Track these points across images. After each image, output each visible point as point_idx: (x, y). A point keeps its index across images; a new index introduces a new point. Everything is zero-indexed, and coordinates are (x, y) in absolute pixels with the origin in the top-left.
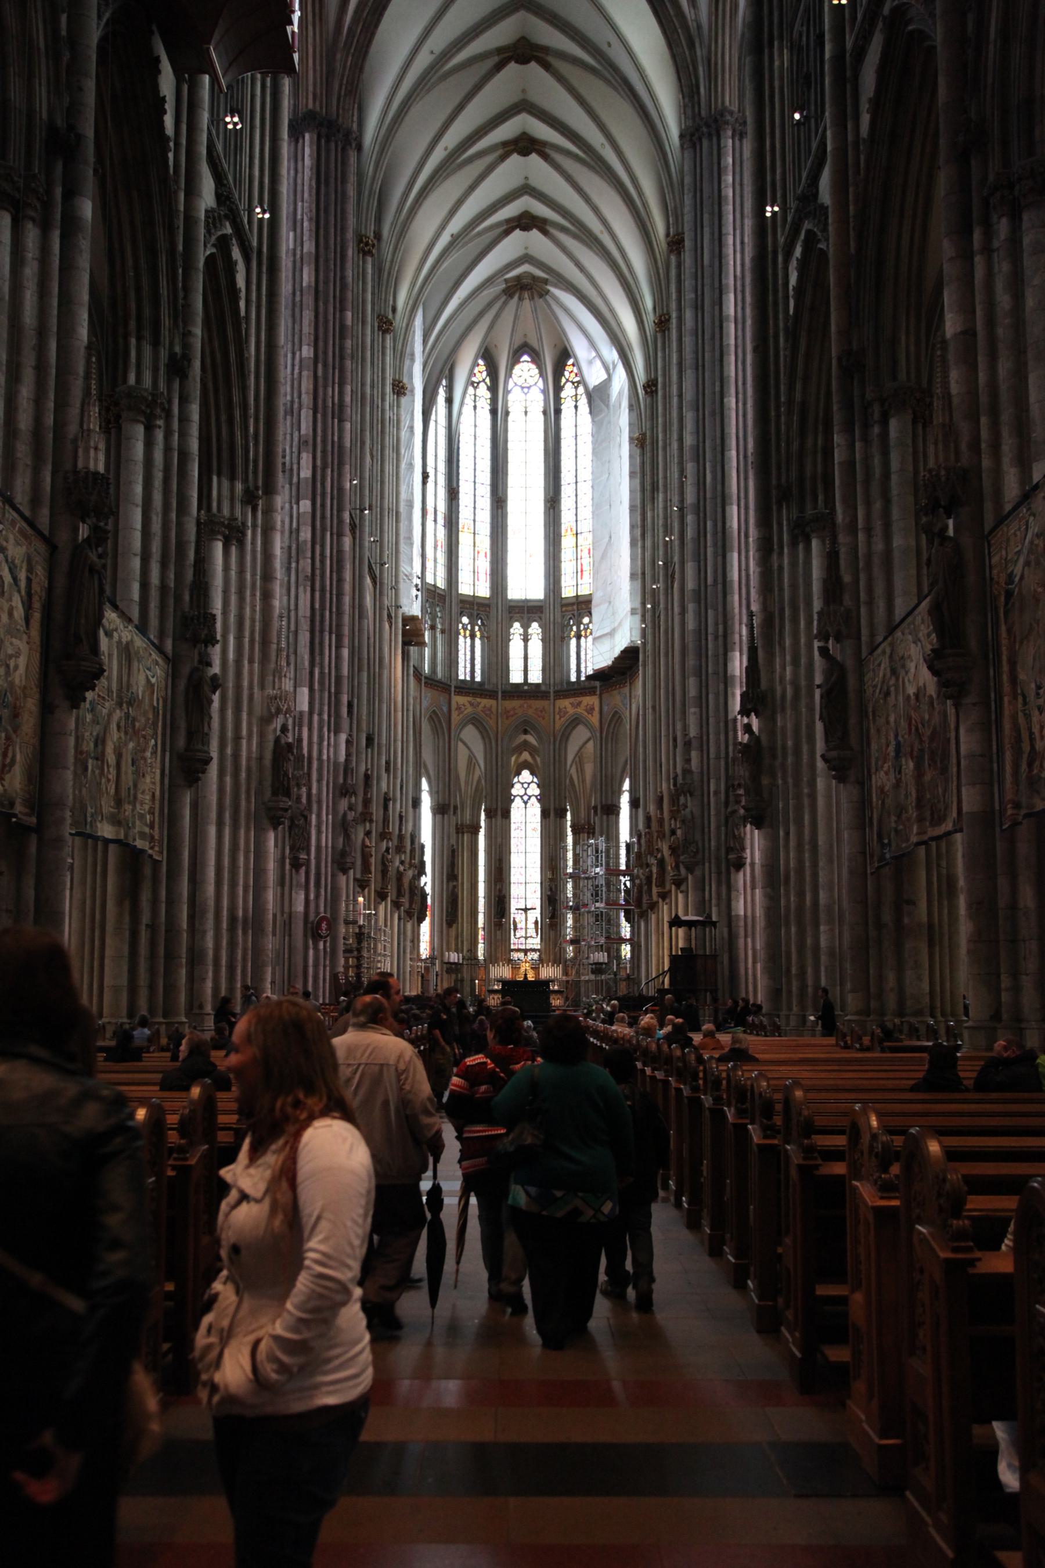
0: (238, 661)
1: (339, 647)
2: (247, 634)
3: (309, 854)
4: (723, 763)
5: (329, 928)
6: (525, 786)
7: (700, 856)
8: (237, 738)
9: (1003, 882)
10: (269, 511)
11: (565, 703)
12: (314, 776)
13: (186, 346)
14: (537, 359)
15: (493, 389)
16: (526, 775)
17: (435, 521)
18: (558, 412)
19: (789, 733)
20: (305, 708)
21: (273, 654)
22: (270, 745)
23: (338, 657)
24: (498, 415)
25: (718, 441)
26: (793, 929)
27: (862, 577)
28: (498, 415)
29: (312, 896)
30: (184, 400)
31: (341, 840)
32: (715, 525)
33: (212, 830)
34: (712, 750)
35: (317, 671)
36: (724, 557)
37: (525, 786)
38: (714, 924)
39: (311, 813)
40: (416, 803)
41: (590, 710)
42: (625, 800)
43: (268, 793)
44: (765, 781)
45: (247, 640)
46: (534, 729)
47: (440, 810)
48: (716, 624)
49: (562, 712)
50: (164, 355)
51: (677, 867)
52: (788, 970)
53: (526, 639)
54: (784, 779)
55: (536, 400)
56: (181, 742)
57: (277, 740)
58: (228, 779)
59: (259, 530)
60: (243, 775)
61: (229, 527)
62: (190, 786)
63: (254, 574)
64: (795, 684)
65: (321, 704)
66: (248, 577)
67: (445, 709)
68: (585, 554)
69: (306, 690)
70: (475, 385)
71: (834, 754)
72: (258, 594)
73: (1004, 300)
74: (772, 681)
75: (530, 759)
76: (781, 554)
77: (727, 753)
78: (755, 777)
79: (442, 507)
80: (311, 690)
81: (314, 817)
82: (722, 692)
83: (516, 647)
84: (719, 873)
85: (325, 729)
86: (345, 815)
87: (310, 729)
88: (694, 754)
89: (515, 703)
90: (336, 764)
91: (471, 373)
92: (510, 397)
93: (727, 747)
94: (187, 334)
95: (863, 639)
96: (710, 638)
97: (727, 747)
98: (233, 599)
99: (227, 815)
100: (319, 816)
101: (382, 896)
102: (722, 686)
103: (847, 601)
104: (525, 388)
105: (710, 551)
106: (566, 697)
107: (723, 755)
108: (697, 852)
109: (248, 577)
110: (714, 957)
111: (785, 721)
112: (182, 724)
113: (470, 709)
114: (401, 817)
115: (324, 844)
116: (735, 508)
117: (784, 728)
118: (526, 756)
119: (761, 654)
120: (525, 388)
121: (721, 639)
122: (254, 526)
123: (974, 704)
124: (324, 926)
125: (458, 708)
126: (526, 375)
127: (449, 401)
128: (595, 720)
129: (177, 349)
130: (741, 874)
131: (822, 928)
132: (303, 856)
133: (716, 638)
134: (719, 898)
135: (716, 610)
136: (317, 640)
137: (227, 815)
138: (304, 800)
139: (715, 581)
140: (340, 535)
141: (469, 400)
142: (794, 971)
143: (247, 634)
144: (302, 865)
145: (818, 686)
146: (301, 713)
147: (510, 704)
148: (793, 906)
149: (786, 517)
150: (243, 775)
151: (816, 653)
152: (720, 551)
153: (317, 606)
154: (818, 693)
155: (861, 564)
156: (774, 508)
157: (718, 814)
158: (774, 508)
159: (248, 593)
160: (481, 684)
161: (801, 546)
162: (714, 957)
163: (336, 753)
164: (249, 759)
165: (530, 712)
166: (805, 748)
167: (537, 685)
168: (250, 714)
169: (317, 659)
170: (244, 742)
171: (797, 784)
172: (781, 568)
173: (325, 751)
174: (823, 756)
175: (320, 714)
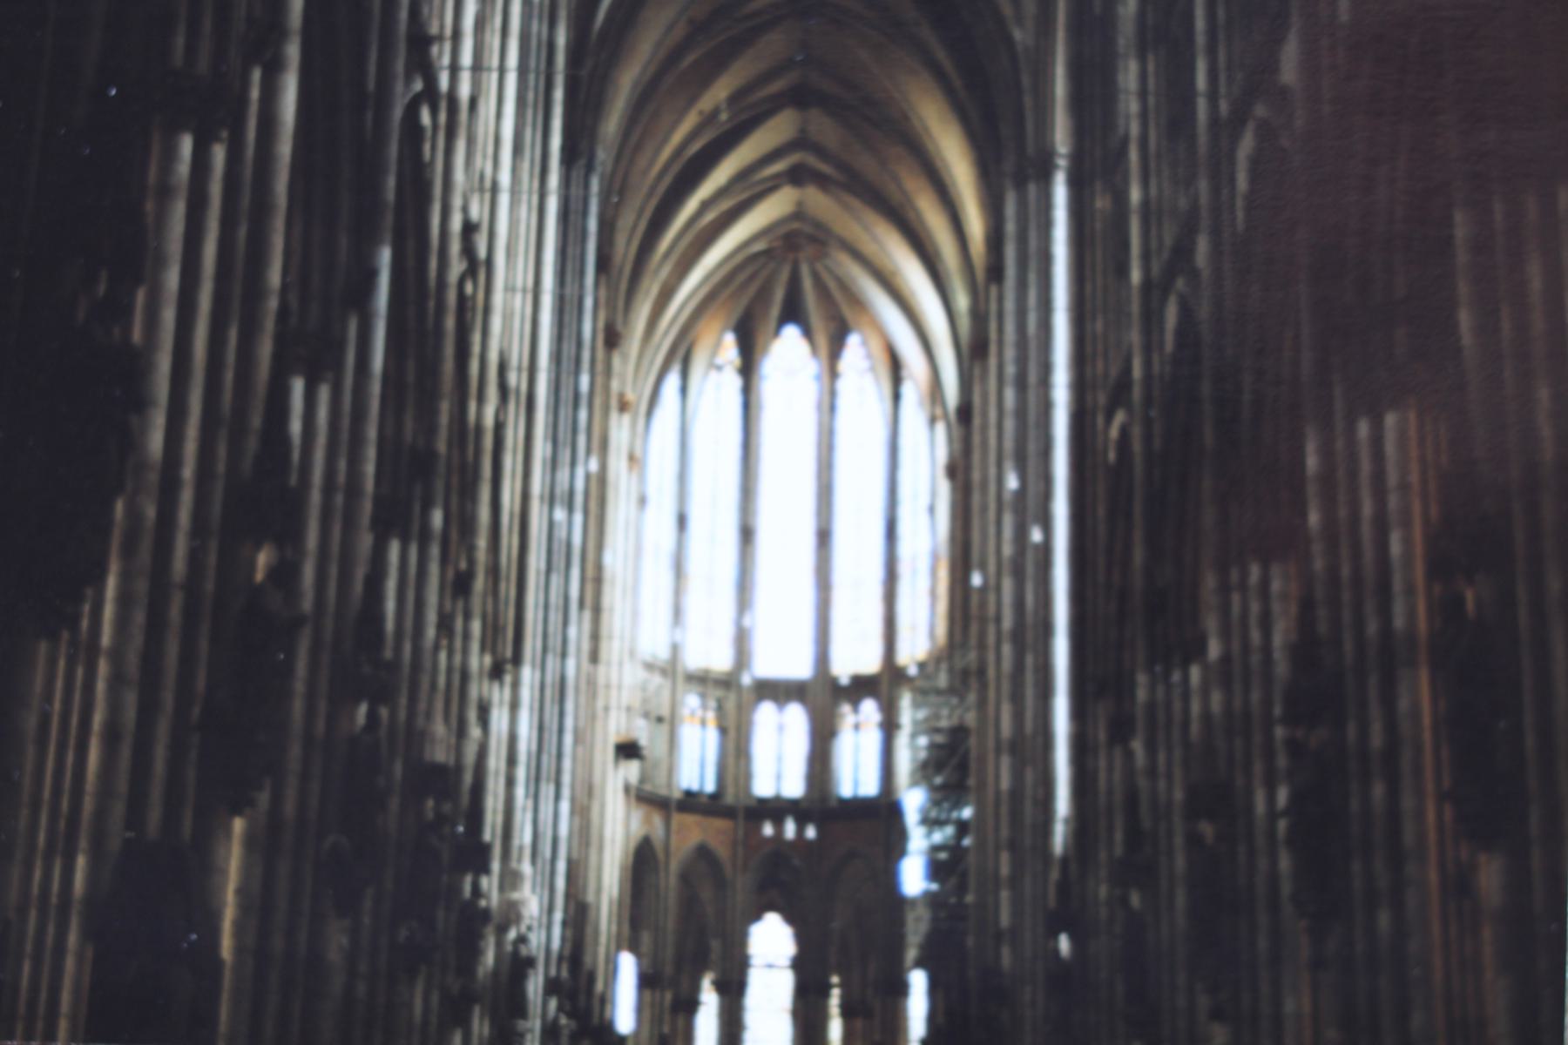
1: (557, 797)
6: (771, 942)
10: (516, 685)
13: (472, 562)
14: (808, 333)
18: (832, 408)
30: (467, 616)
37: (771, 942)
47: (646, 981)
50: (450, 574)
73: (1255, 636)
94: (471, 549)
127: (684, 390)
129: (463, 565)
140: (564, 655)
160: (715, 797)
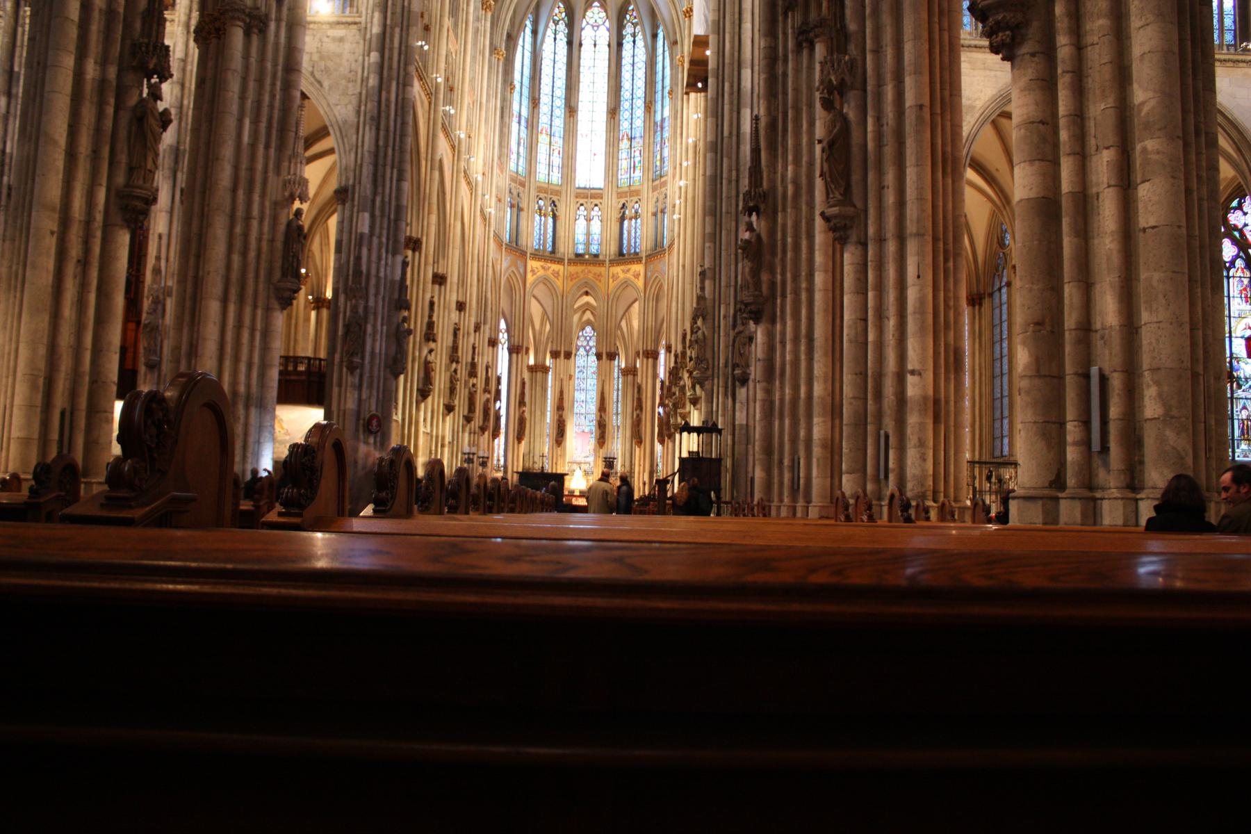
0: (253, 146)
2: (264, 119)
3: (363, 358)
4: (732, 289)
5: (379, 425)
7: (710, 372)
8: (248, 218)
9: (1070, 292)
11: (618, 270)
12: (372, 291)
15: (571, 25)
16: (588, 329)
17: (519, 123)
19: (790, 231)
20: (366, 230)
21: (291, 141)
22: (282, 228)
23: (399, 189)
24: (573, 44)
25: (737, 16)
26: (787, 422)
27: (868, 24)
28: (573, 44)
29: (364, 396)
31: (393, 349)
32: (732, 86)
33: (214, 307)
34: (723, 278)
35: (378, 199)
36: (739, 113)
38: (719, 432)
39: (366, 323)
40: (493, 343)
41: (637, 276)
42: (662, 352)
43: (277, 275)
44: (765, 277)
45: (263, 125)
46: (592, 288)
48: (730, 170)
49: (615, 277)
51: (693, 387)
52: (781, 462)
53: (588, 220)
54: (783, 274)
55: (604, 36)
56: (120, 179)
57: (289, 224)
58: (236, 258)
59: (283, 24)
60: (252, 254)
61: (249, 15)
62: (283, 309)
63: (275, 65)
64: (796, 182)
65: (381, 228)
66: (269, 65)
67: (522, 270)
68: (637, 153)
69: (367, 215)
70: (556, 23)
71: (835, 210)
72: (279, 84)
74: (772, 181)
75: (592, 318)
76: (786, 61)
77: (736, 282)
78: (756, 273)
79: (525, 113)
80: (373, 216)
81: (369, 328)
82: (733, 229)
83: (581, 225)
84: (726, 387)
85: (383, 251)
86: (398, 326)
87: (370, 250)
88: (707, 283)
89: (579, 268)
90: (393, 282)
91: (552, 9)
92: (583, 33)
93: (736, 277)
95: (869, 88)
96: (724, 182)
97: (736, 277)
98: (252, 85)
99: (233, 291)
100: (374, 326)
101: (449, 409)
102: (733, 224)
103: (853, 49)
104: (596, 27)
105: (726, 107)
106: (618, 264)
107: (733, 283)
108: (707, 369)
109: (269, 65)
110: (719, 460)
111: (786, 219)
112: (123, 158)
113: (541, 273)
114: (474, 348)
115: (377, 351)
116: (749, 71)
117: (784, 226)
118: (588, 315)
119: (763, 154)
120: (596, 27)
121: (734, 183)
122: (278, 20)
123: (1033, 55)
124: (375, 422)
125: (532, 271)
126: (596, 17)
127: (535, 32)
128: (640, 283)
130: (744, 390)
131: (816, 420)
132: (357, 360)
133: (730, 182)
134: (724, 409)
135: (730, 158)
136: (379, 174)
137: (233, 291)
138: (361, 310)
139: (731, 133)
141: (550, 33)
142: (786, 462)
143: (264, 119)
144: (356, 368)
145: (820, 142)
146: (362, 235)
147: (573, 269)
148: (787, 397)
149: (792, 23)
150: (252, 254)
151: (818, 105)
152: (735, 108)
153: (381, 143)
154: (818, 148)
155: (868, 11)
156: (780, 18)
157: (727, 335)
158: (780, 18)
159: (268, 81)
161: (805, 52)
162: (719, 460)
163: (393, 273)
164: (260, 240)
165: (590, 276)
166: (804, 243)
167: (596, 256)
168: (263, 195)
169: (380, 189)
170: (255, 223)
171: (796, 277)
172: (785, 75)
173: (382, 270)
174: (822, 214)
175: (380, 237)
